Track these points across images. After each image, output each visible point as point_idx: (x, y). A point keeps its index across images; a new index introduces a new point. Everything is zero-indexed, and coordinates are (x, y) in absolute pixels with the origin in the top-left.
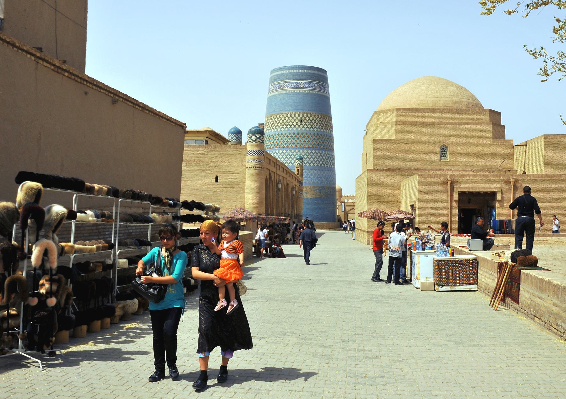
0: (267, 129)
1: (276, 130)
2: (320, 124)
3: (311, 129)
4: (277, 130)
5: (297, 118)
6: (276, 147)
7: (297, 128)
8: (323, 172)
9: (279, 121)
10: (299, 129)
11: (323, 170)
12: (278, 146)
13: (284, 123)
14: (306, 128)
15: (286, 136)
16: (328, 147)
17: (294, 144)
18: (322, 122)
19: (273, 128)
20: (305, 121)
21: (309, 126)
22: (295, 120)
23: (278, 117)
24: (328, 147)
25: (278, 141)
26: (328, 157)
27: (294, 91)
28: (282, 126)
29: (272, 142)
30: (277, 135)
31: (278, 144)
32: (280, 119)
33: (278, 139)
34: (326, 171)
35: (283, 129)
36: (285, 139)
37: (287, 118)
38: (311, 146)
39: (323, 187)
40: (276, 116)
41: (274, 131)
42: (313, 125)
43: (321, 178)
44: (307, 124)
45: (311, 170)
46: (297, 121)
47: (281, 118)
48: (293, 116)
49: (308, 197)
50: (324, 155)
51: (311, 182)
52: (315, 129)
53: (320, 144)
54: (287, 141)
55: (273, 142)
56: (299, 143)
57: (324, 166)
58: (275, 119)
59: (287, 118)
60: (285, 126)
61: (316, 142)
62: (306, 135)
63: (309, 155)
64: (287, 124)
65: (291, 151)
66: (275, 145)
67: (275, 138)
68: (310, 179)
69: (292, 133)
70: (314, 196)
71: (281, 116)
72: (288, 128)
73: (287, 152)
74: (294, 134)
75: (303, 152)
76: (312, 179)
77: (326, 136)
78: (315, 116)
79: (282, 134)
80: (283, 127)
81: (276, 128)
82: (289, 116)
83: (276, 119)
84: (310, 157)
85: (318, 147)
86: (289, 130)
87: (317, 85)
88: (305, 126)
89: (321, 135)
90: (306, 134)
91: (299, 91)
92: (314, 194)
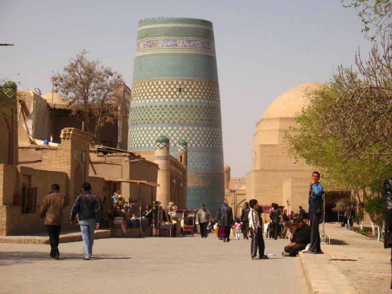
0: (136, 98)
1: (147, 101)
2: (204, 93)
3: (193, 100)
4: (150, 101)
5: (175, 86)
6: (148, 123)
7: (175, 100)
9: (152, 90)
10: (178, 100)
11: (207, 152)
12: (151, 122)
13: (159, 92)
14: (186, 99)
15: (160, 109)
16: (213, 122)
17: (171, 119)
18: (206, 90)
19: (144, 99)
20: (185, 90)
21: (191, 97)
22: (172, 89)
23: (151, 84)
24: (213, 122)
25: (151, 116)
26: (214, 136)
27: (170, 52)
28: (156, 96)
29: (143, 116)
30: (149, 108)
31: (151, 119)
32: (153, 87)
33: (151, 113)
35: (157, 100)
36: (160, 113)
37: (162, 87)
38: (192, 122)
40: (148, 83)
41: (145, 102)
43: (205, 162)
44: (188, 93)
45: (193, 151)
46: (175, 90)
47: (155, 86)
48: (170, 83)
52: (198, 101)
54: (163, 116)
55: (145, 116)
56: (177, 119)
58: (146, 87)
59: (162, 87)
60: (159, 97)
61: (199, 116)
62: (187, 107)
63: (191, 133)
64: (162, 93)
65: (167, 129)
66: (146, 119)
67: (147, 111)
68: (192, 163)
69: (169, 105)
70: (196, 185)
71: (155, 83)
72: (164, 100)
73: (162, 129)
74: (171, 106)
75: (183, 129)
78: (197, 83)
79: (156, 107)
80: (158, 98)
81: (148, 98)
82: (165, 83)
83: (148, 87)
84: (191, 135)
85: (202, 122)
86: (164, 101)
88: (186, 97)
90: (187, 106)
91: (178, 52)
92: (196, 183)
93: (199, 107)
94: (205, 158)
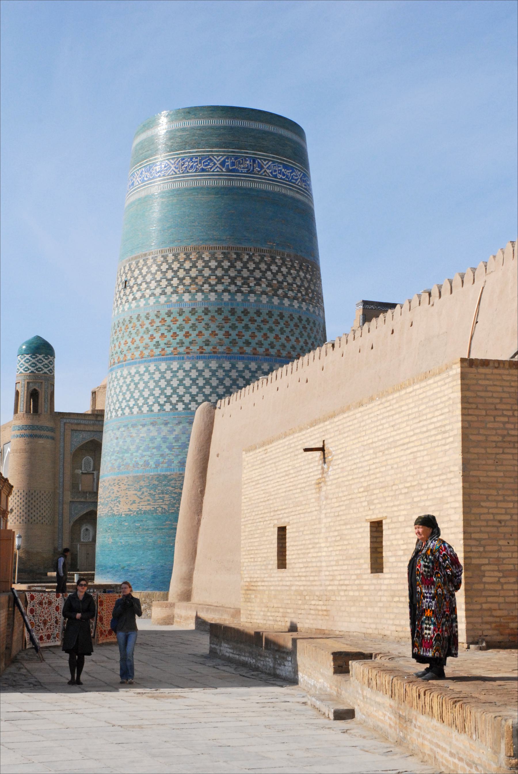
8: (165, 430)
11: (166, 424)
34: (180, 423)
38: (137, 354)
39: (166, 476)
44: (135, 289)
51: (131, 465)
53: (162, 343)
61: (152, 337)
68: (129, 455)
70: (134, 507)
76: (132, 454)
77: (187, 314)
87: (175, 163)
89: (169, 314)
92: (134, 502)
93: (152, 316)
94: (159, 439)
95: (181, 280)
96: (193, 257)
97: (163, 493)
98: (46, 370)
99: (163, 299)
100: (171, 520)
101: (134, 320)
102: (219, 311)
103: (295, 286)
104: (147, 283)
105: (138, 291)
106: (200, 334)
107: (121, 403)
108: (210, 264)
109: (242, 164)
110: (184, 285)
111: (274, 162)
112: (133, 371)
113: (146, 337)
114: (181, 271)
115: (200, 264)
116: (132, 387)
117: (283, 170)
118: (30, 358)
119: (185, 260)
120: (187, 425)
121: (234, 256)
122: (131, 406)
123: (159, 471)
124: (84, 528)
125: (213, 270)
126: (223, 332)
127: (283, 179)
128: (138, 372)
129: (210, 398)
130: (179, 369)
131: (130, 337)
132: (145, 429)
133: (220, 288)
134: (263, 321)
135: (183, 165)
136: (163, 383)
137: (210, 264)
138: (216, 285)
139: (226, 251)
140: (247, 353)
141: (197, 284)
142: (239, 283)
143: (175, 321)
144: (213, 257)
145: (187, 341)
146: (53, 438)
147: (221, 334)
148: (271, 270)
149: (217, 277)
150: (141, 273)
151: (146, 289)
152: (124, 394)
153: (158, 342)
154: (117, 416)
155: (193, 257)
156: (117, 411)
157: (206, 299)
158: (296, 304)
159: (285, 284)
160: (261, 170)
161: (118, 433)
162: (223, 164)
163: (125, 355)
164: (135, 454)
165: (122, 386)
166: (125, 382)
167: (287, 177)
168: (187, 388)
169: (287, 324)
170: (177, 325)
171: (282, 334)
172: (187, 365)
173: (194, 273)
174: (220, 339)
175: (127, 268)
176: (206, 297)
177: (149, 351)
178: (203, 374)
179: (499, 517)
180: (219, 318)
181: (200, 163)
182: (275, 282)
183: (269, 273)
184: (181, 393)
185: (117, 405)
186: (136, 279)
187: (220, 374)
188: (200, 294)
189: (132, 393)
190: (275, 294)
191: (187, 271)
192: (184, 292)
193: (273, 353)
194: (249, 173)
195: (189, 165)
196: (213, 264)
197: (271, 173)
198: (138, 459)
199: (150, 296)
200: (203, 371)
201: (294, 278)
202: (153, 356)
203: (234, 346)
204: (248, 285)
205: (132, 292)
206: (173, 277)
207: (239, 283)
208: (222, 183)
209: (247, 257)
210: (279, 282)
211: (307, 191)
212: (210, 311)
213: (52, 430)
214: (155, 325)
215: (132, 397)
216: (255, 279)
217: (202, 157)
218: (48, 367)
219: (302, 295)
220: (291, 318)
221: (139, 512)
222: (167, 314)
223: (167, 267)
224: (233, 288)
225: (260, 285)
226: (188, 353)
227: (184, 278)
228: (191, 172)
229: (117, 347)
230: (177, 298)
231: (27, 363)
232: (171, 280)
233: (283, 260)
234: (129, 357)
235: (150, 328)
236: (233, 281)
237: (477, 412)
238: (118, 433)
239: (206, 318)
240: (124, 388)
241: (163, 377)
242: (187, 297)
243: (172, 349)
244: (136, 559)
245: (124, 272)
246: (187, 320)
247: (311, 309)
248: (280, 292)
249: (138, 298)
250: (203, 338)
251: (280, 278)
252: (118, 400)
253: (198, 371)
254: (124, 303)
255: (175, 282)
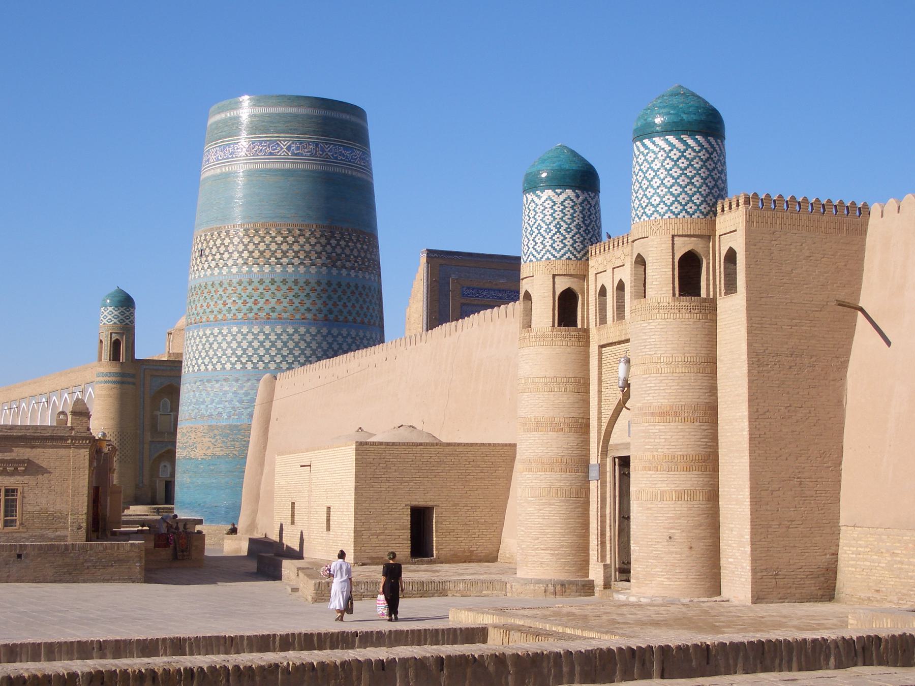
11: (237, 380)
34: (249, 380)
38: (212, 317)
39: (236, 426)
42: (222, 258)
44: (210, 258)
49: (198, 455)
50: (244, 339)
52: (290, 269)
57: (244, 367)
61: (225, 304)
68: (204, 406)
70: (209, 452)
76: (207, 406)
77: (256, 284)
89: (240, 283)
92: (209, 448)
95: (251, 253)
96: (261, 233)
97: (234, 441)
98: (127, 321)
99: (234, 270)
100: (240, 465)
101: (210, 287)
102: (284, 282)
103: (352, 257)
104: (221, 254)
105: (212, 260)
106: (267, 302)
107: (197, 360)
108: (276, 239)
109: (306, 148)
110: (253, 257)
111: (335, 145)
112: (208, 332)
113: (220, 302)
114: (251, 244)
115: (268, 239)
116: (207, 346)
117: (343, 152)
118: (113, 310)
119: (255, 235)
120: (255, 382)
121: (298, 232)
122: (206, 363)
123: (231, 422)
124: (162, 464)
125: (279, 245)
126: (287, 300)
127: (344, 160)
128: (212, 334)
129: (275, 359)
130: (248, 332)
131: (205, 302)
132: (219, 384)
133: (285, 261)
134: (322, 290)
135: (253, 149)
136: (234, 345)
137: (276, 239)
138: (281, 258)
139: (291, 228)
140: (308, 319)
141: (265, 257)
142: (302, 257)
143: (245, 289)
144: (279, 233)
145: (255, 308)
146: (134, 384)
147: (285, 302)
148: (331, 244)
149: (282, 251)
150: (215, 245)
151: (220, 259)
152: (200, 353)
153: (230, 308)
154: (193, 371)
155: (261, 233)
156: (193, 367)
157: (273, 271)
158: (353, 273)
159: (343, 256)
160: (323, 153)
161: (195, 387)
162: (289, 148)
163: (201, 317)
164: (209, 406)
165: (198, 345)
166: (201, 342)
167: (347, 158)
168: (256, 350)
169: (344, 292)
170: (247, 293)
171: (340, 301)
172: (256, 330)
173: (262, 247)
174: (285, 307)
175: (203, 238)
176: (273, 268)
177: (222, 315)
178: (270, 337)
179: (370, 510)
180: (284, 288)
181: (269, 147)
182: (334, 254)
183: (329, 247)
184: (250, 354)
185: (194, 362)
186: (211, 249)
187: (285, 337)
188: (267, 266)
189: (207, 352)
190: (334, 266)
191: (257, 245)
192: (253, 264)
193: (331, 319)
194: (313, 157)
195: (258, 149)
196: (279, 239)
197: (332, 155)
198: (212, 411)
199: (223, 266)
200: (270, 334)
201: (352, 250)
202: (225, 320)
203: (297, 313)
204: (310, 258)
205: (207, 261)
206: (243, 250)
207: (302, 257)
208: (288, 166)
209: (310, 233)
210: (337, 255)
211: (366, 168)
212: (275, 282)
213: (133, 376)
214: (228, 293)
215: (207, 355)
216: (316, 253)
217: (271, 142)
218: (130, 318)
219: (359, 265)
220: (348, 286)
221: (214, 457)
222: (238, 283)
223: (238, 240)
224: (296, 261)
225: (320, 258)
226: (256, 319)
227: (253, 252)
228: (261, 156)
229: (194, 309)
230: (247, 269)
231: (110, 315)
232: (242, 252)
233: (342, 234)
234: (204, 320)
235: (223, 295)
236: (296, 253)
237: (362, 465)
238: (195, 387)
239: (273, 288)
240: (200, 347)
241: (234, 339)
242: (255, 269)
243: (242, 314)
244: (210, 496)
245: (200, 241)
246: (256, 289)
247: (367, 277)
248: (339, 263)
249: (213, 267)
250: (270, 306)
251: (339, 251)
252: (194, 357)
253: (265, 334)
254: (200, 270)
255: (246, 254)
